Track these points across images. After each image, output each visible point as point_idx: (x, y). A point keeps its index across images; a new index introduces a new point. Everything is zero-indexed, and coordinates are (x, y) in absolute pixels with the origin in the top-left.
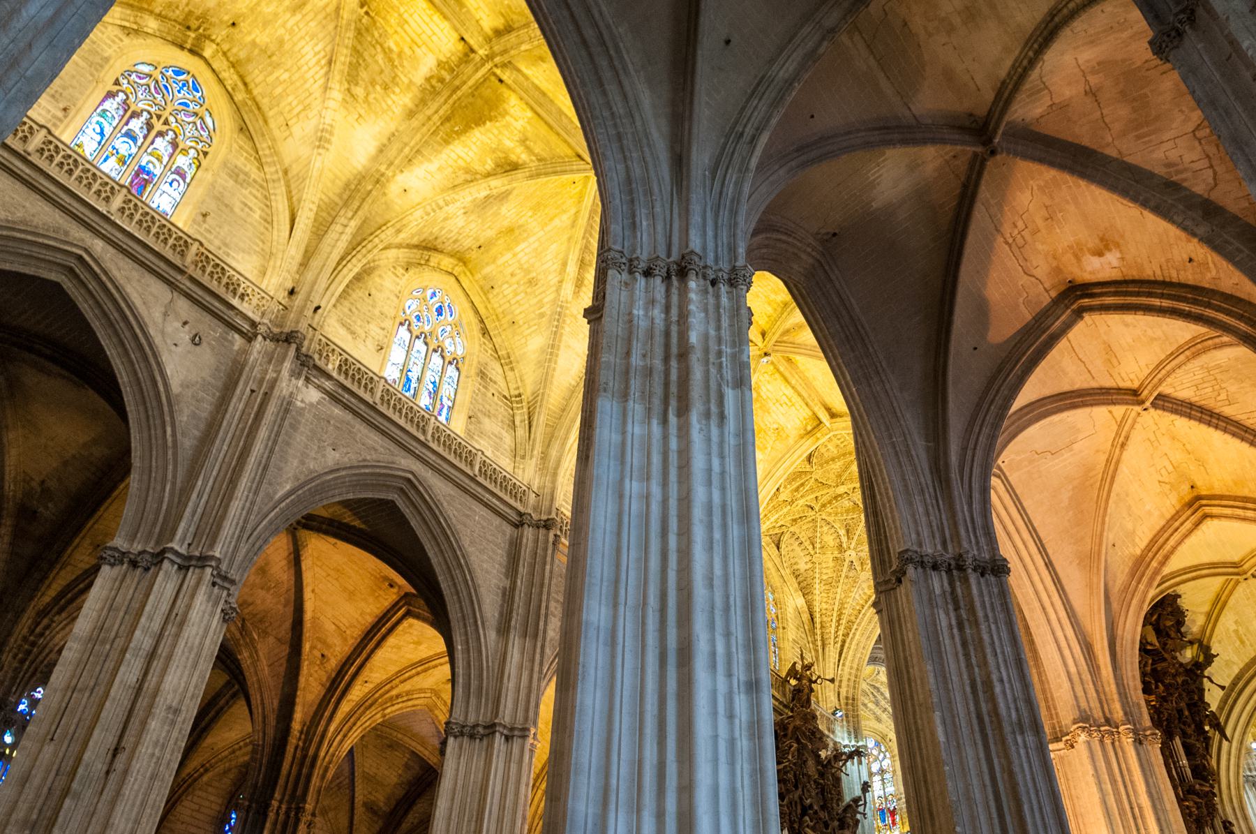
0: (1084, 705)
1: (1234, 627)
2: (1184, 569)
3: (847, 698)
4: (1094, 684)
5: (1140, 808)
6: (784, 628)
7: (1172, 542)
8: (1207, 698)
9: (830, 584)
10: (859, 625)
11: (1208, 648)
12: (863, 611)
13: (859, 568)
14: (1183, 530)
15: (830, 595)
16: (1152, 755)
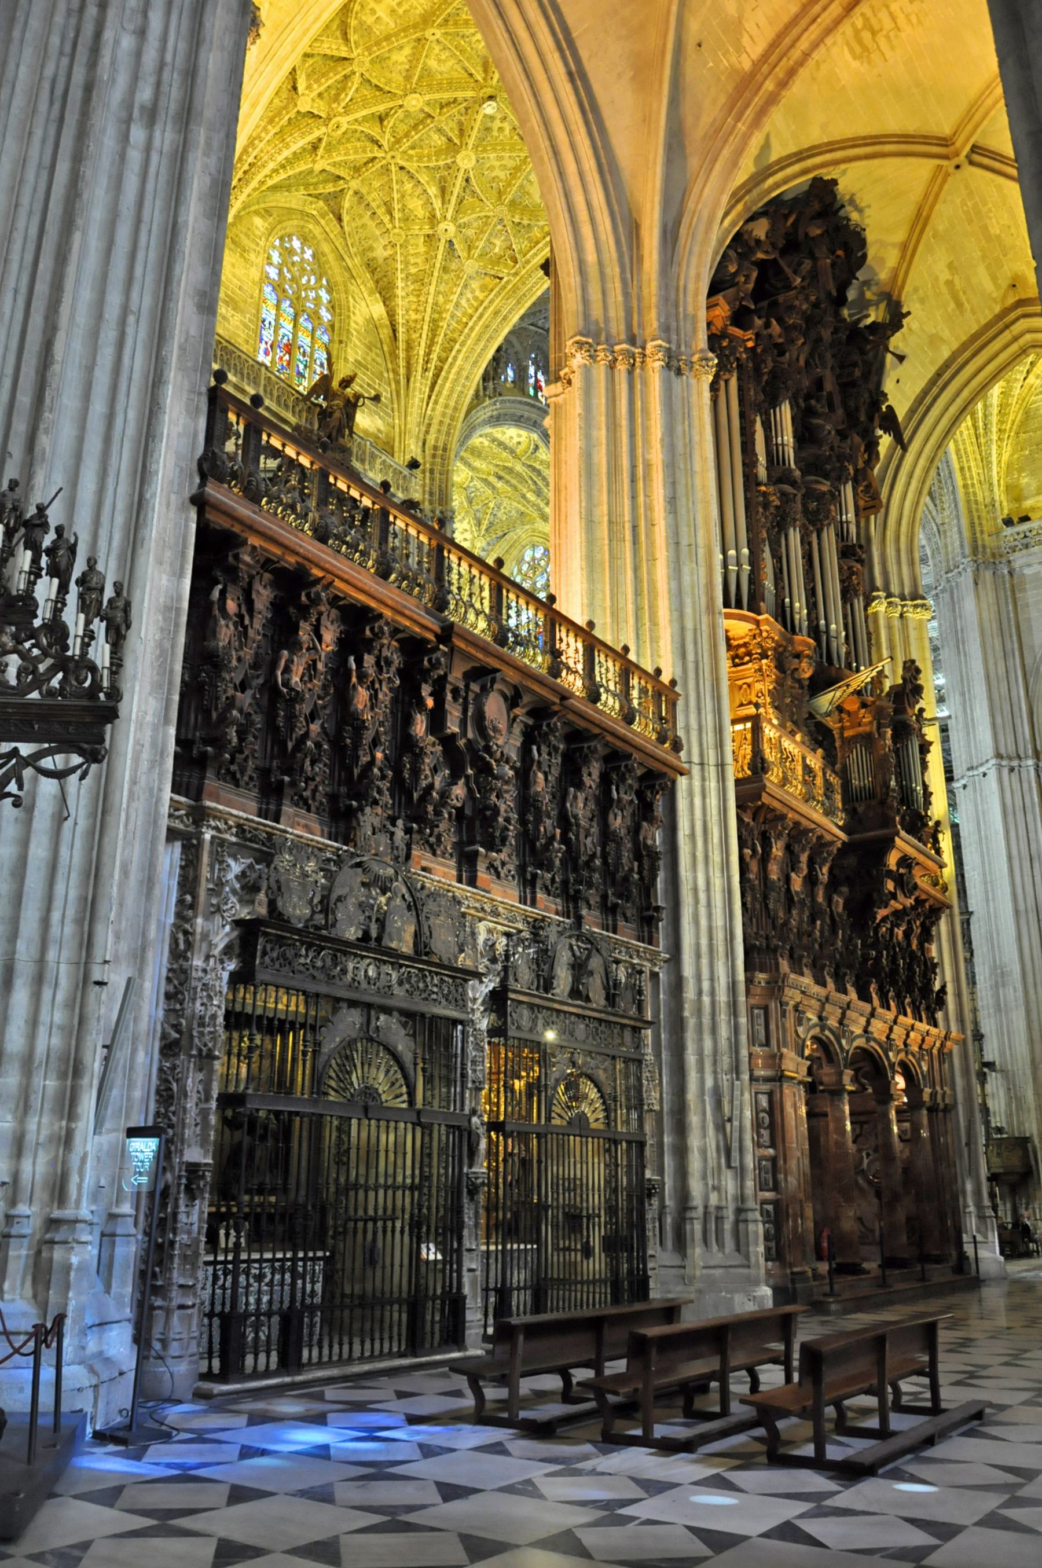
0: (597, 312)
1: (945, 275)
2: (853, 139)
3: (435, 448)
4: (624, 281)
5: (648, 466)
6: (341, 342)
7: (804, 44)
8: (888, 386)
9: (420, 280)
10: (463, 344)
11: (898, 305)
12: (471, 324)
13: (463, 254)
14: (826, 19)
15: (422, 299)
16: (694, 391)
